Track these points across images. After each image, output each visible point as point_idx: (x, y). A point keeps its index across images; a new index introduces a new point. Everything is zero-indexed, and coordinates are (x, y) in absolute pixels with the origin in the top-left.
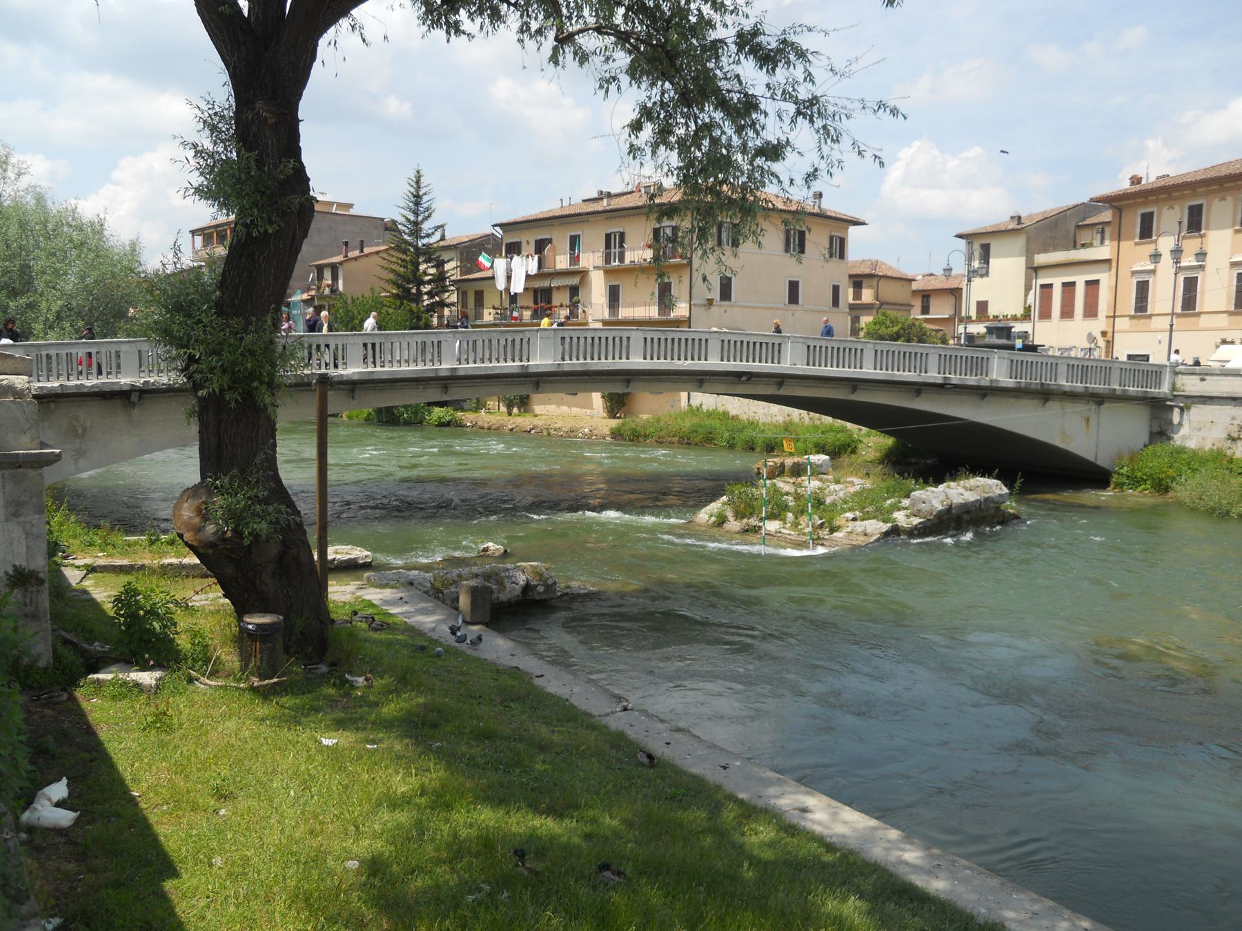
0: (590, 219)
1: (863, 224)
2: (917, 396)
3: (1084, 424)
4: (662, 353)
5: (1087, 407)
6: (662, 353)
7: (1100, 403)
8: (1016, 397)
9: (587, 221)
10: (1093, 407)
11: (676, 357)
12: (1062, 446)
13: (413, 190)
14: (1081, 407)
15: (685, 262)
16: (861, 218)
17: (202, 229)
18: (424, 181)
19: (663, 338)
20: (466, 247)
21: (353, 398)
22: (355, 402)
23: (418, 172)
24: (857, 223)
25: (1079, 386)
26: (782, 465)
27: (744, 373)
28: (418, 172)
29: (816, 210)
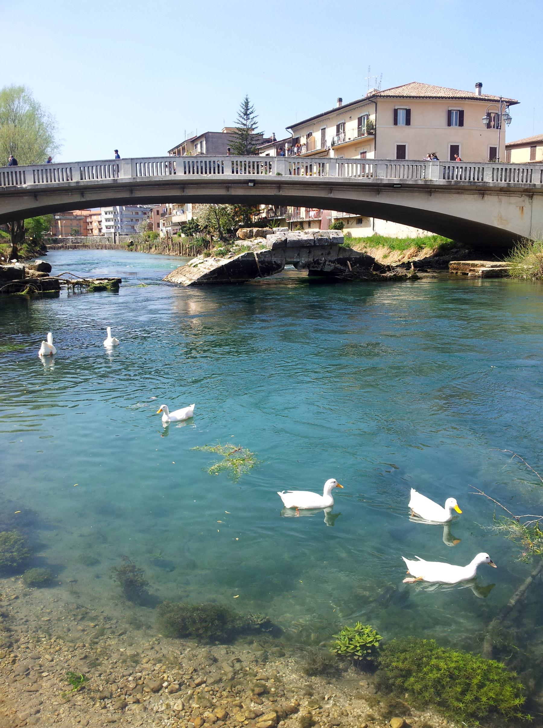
0: (330, 117)
1: (516, 103)
2: (379, 194)
3: (518, 211)
4: (196, 170)
5: (522, 199)
6: (196, 170)
7: (531, 197)
8: (458, 193)
9: (329, 119)
10: (527, 199)
11: (204, 172)
12: (499, 227)
13: (243, 110)
14: (515, 200)
15: (372, 137)
16: (514, 99)
17: (172, 150)
18: (250, 105)
19: (195, 161)
20: (280, 144)
21: (37, 200)
22: (38, 202)
23: (247, 100)
24: (511, 103)
25: (503, 183)
26: (251, 231)
27: (251, 181)
28: (247, 100)
29: (476, 95)
